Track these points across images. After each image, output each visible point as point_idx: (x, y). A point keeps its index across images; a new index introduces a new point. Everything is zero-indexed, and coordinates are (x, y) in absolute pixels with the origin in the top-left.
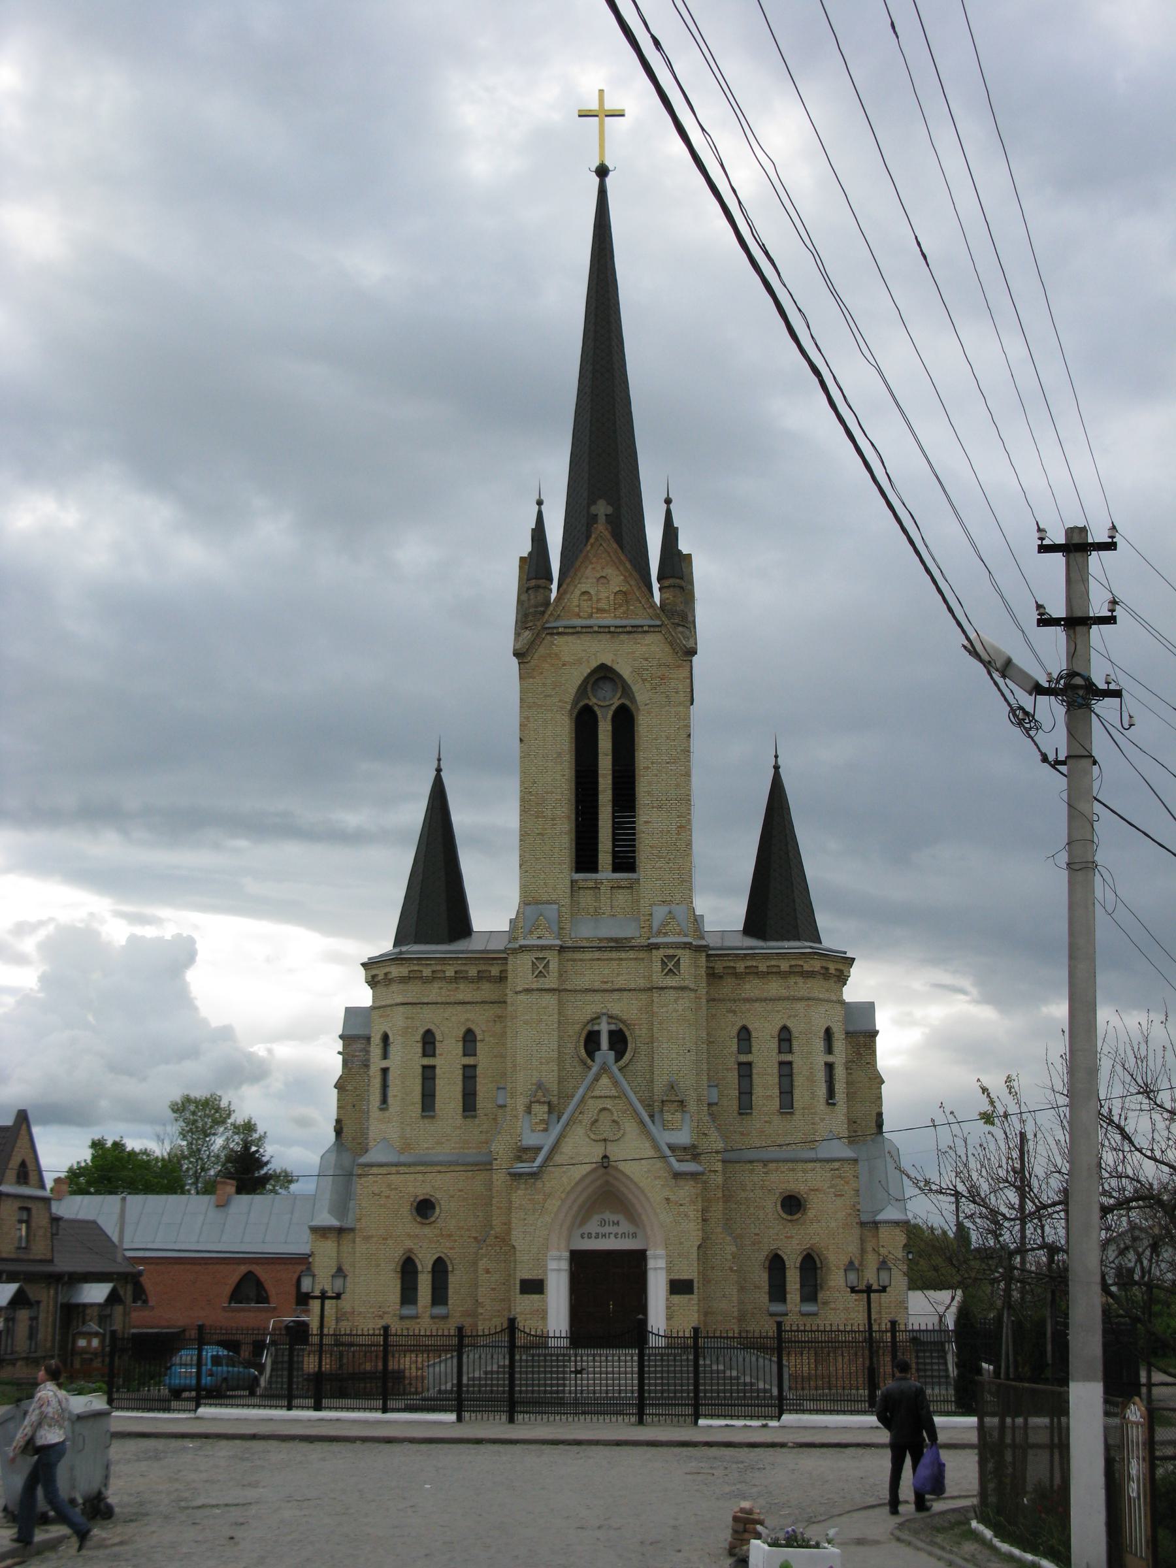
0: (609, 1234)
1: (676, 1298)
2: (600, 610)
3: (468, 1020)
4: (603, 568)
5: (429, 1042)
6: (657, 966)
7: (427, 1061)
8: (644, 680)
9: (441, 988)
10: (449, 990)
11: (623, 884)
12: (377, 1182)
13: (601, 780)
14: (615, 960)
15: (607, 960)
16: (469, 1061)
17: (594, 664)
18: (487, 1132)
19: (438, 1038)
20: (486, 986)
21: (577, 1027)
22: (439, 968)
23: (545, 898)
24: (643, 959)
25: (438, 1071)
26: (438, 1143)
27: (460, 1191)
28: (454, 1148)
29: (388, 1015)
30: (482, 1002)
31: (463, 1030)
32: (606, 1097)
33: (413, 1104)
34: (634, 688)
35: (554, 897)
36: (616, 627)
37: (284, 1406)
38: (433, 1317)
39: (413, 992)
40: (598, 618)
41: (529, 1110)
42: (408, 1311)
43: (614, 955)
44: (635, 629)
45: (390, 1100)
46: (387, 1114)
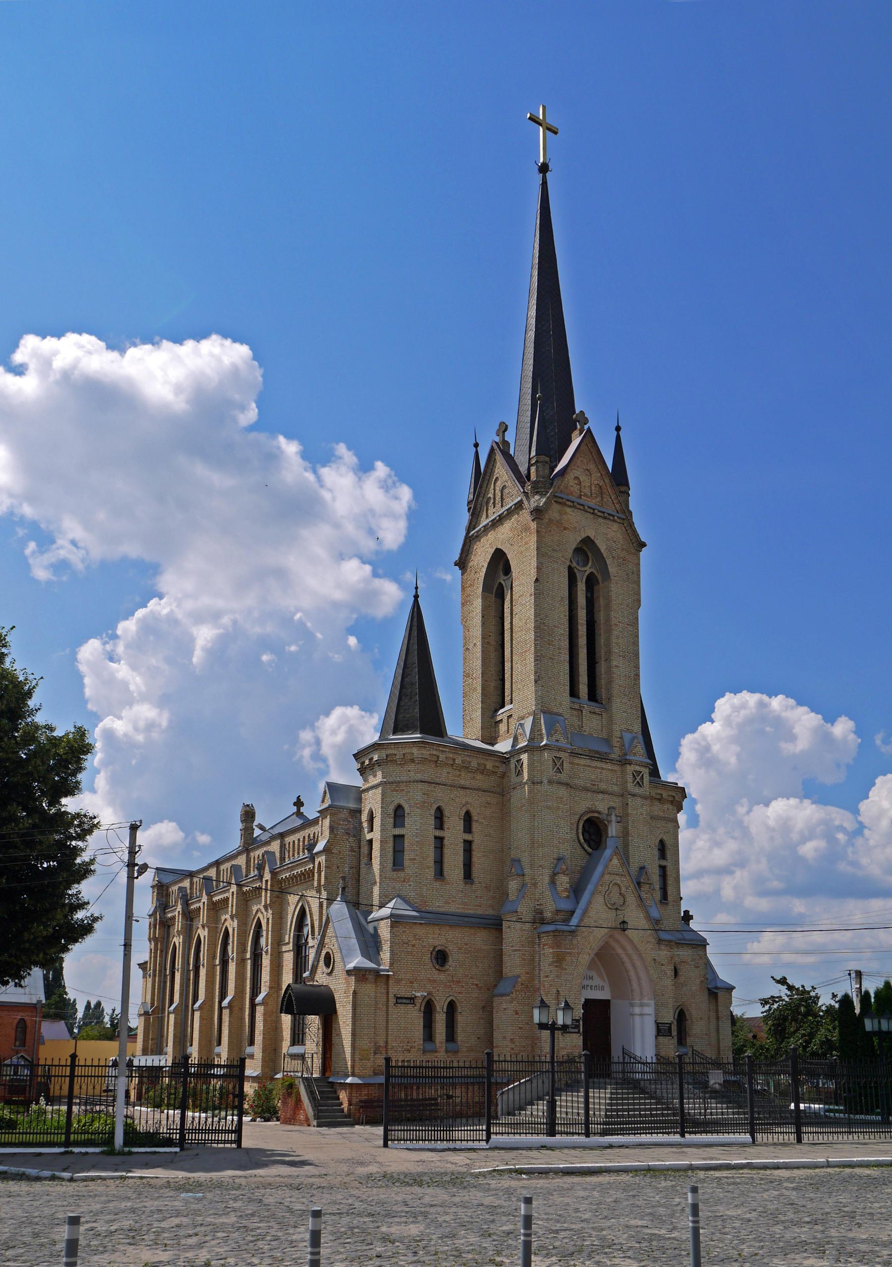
0: (587, 986)
1: (661, 1039)
2: (585, 495)
3: (467, 803)
4: (588, 464)
5: (440, 818)
6: (630, 778)
7: (438, 833)
8: (614, 558)
9: (448, 773)
10: (455, 776)
11: (597, 710)
12: (405, 932)
13: (580, 627)
14: (599, 768)
15: (594, 767)
16: (468, 837)
17: (583, 536)
18: (481, 897)
19: (446, 813)
20: (479, 777)
21: (577, 817)
22: (451, 756)
23: (555, 710)
24: (615, 771)
25: (446, 842)
26: (446, 903)
27: (466, 944)
28: (458, 908)
29: (403, 790)
30: (478, 789)
31: (464, 811)
32: (617, 875)
33: (428, 867)
34: (608, 562)
35: (561, 711)
36: (599, 511)
37: (582, 1133)
38: (447, 1051)
39: (429, 772)
40: (585, 500)
41: (553, 882)
42: (429, 1046)
43: (599, 764)
44: (608, 517)
45: (407, 863)
46: (402, 874)
